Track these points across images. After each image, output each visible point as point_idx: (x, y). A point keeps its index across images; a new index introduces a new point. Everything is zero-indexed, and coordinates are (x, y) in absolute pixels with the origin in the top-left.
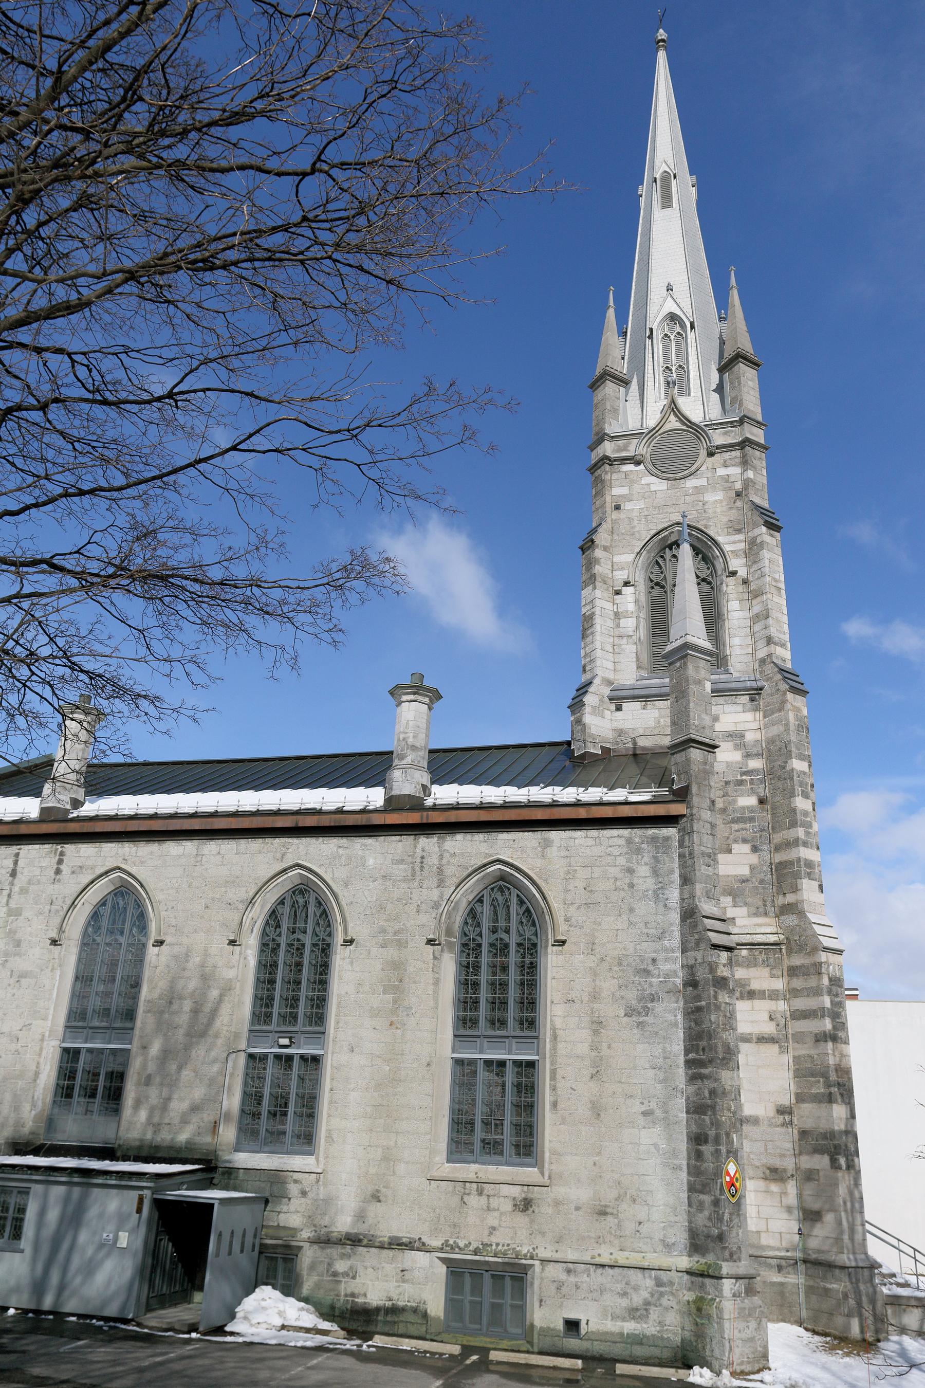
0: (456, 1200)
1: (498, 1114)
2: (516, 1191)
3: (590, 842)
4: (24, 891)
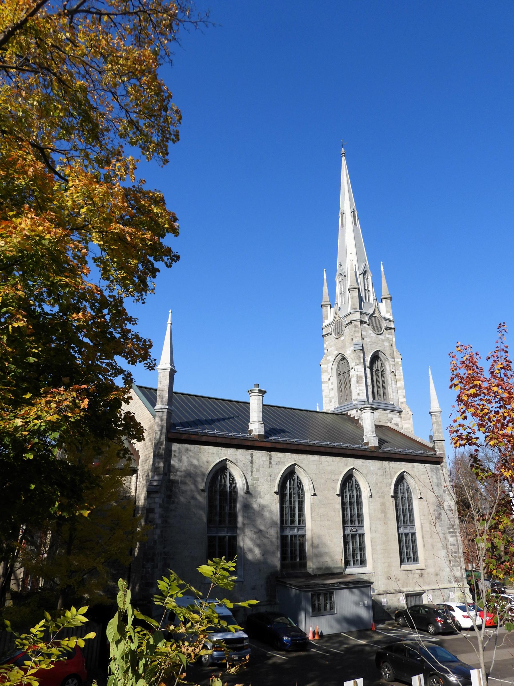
0: (407, 576)
1: (407, 550)
2: (418, 572)
3: (422, 467)
4: (257, 470)
